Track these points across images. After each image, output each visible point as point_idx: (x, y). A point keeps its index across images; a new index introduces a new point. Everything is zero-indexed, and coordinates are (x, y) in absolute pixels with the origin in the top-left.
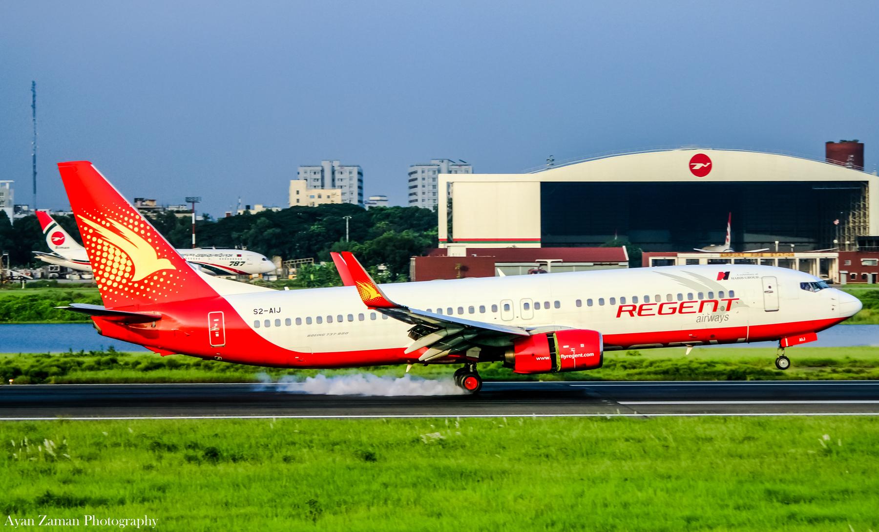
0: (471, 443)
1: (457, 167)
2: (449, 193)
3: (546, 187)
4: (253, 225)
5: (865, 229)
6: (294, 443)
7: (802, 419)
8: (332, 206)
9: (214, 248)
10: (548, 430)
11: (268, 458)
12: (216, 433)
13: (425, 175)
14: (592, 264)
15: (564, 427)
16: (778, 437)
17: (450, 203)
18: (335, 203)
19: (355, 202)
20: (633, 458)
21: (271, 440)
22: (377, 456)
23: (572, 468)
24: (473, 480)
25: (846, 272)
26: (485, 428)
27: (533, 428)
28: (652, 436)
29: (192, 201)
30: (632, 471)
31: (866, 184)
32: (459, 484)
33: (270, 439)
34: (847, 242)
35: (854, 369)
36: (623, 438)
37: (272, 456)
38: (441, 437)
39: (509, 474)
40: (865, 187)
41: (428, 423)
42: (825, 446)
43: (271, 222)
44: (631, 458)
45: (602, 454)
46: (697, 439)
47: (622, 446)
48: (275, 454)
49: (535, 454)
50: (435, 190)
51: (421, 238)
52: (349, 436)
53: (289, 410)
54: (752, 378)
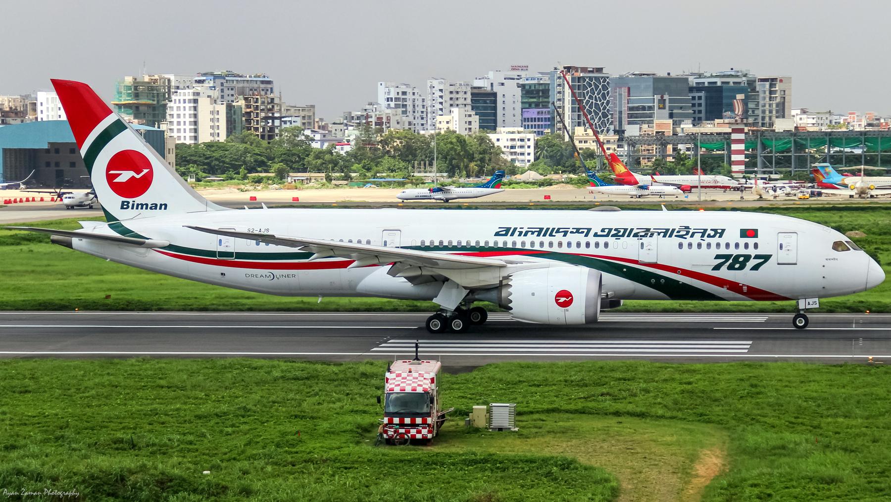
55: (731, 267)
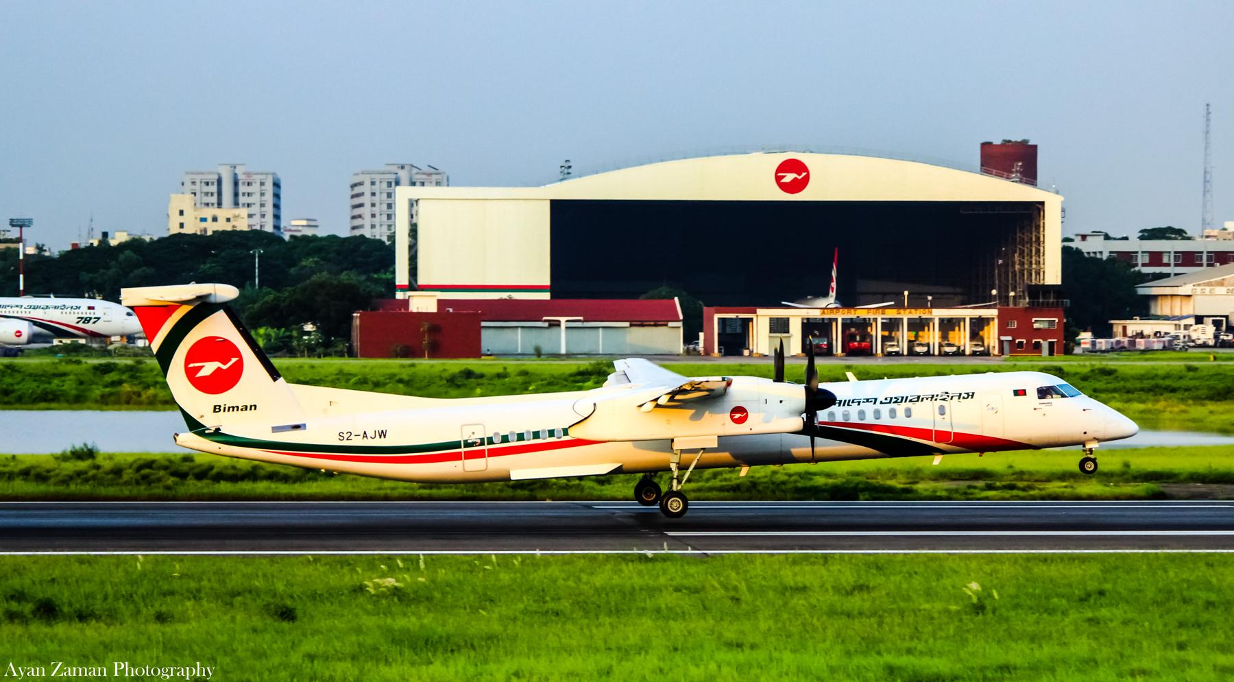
0: (443, 593)
1: (424, 177)
2: (412, 216)
3: (558, 207)
4: (113, 262)
5: (1038, 273)
6: (172, 593)
7: (940, 559)
8: (234, 234)
9: (52, 296)
10: (557, 573)
11: (131, 615)
12: (54, 576)
13: (376, 188)
14: (627, 324)
15: (582, 571)
16: (905, 586)
17: (413, 232)
18: (238, 229)
19: (269, 228)
20: (687, 617)
21: (138, 587)
22: (299, 613)
23: (594, 631)
24: (445, 650)
25: (1010, 338)
26: (463, 571)
27: (536, 571)
28: (717, 585)
29: (20, 224)
30: (685, 636)
31: (1040, 206)
32: (424, 656)
33: (135, 586)
34: (1012, 294)
35: (1020, 484)
36: (671, 586)
37: (138, 612)
38: (397, 584)
39: (498, 641)
40: (1039, 210)
41: (377, 562)
42: (975, 600)
43: (140, 258)
44: (684, 616)
45: (640, 611)
46: (784, 590)
47: (668, 599)
48: (144, 610)
49: (540, 610)
50: (390, 212)
51: (369, 283)
52: (257, 583)
53: (165, 543)
54: (867, 496)
55: (84, 322)
